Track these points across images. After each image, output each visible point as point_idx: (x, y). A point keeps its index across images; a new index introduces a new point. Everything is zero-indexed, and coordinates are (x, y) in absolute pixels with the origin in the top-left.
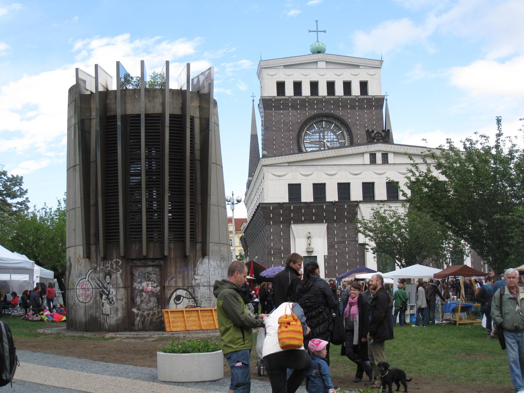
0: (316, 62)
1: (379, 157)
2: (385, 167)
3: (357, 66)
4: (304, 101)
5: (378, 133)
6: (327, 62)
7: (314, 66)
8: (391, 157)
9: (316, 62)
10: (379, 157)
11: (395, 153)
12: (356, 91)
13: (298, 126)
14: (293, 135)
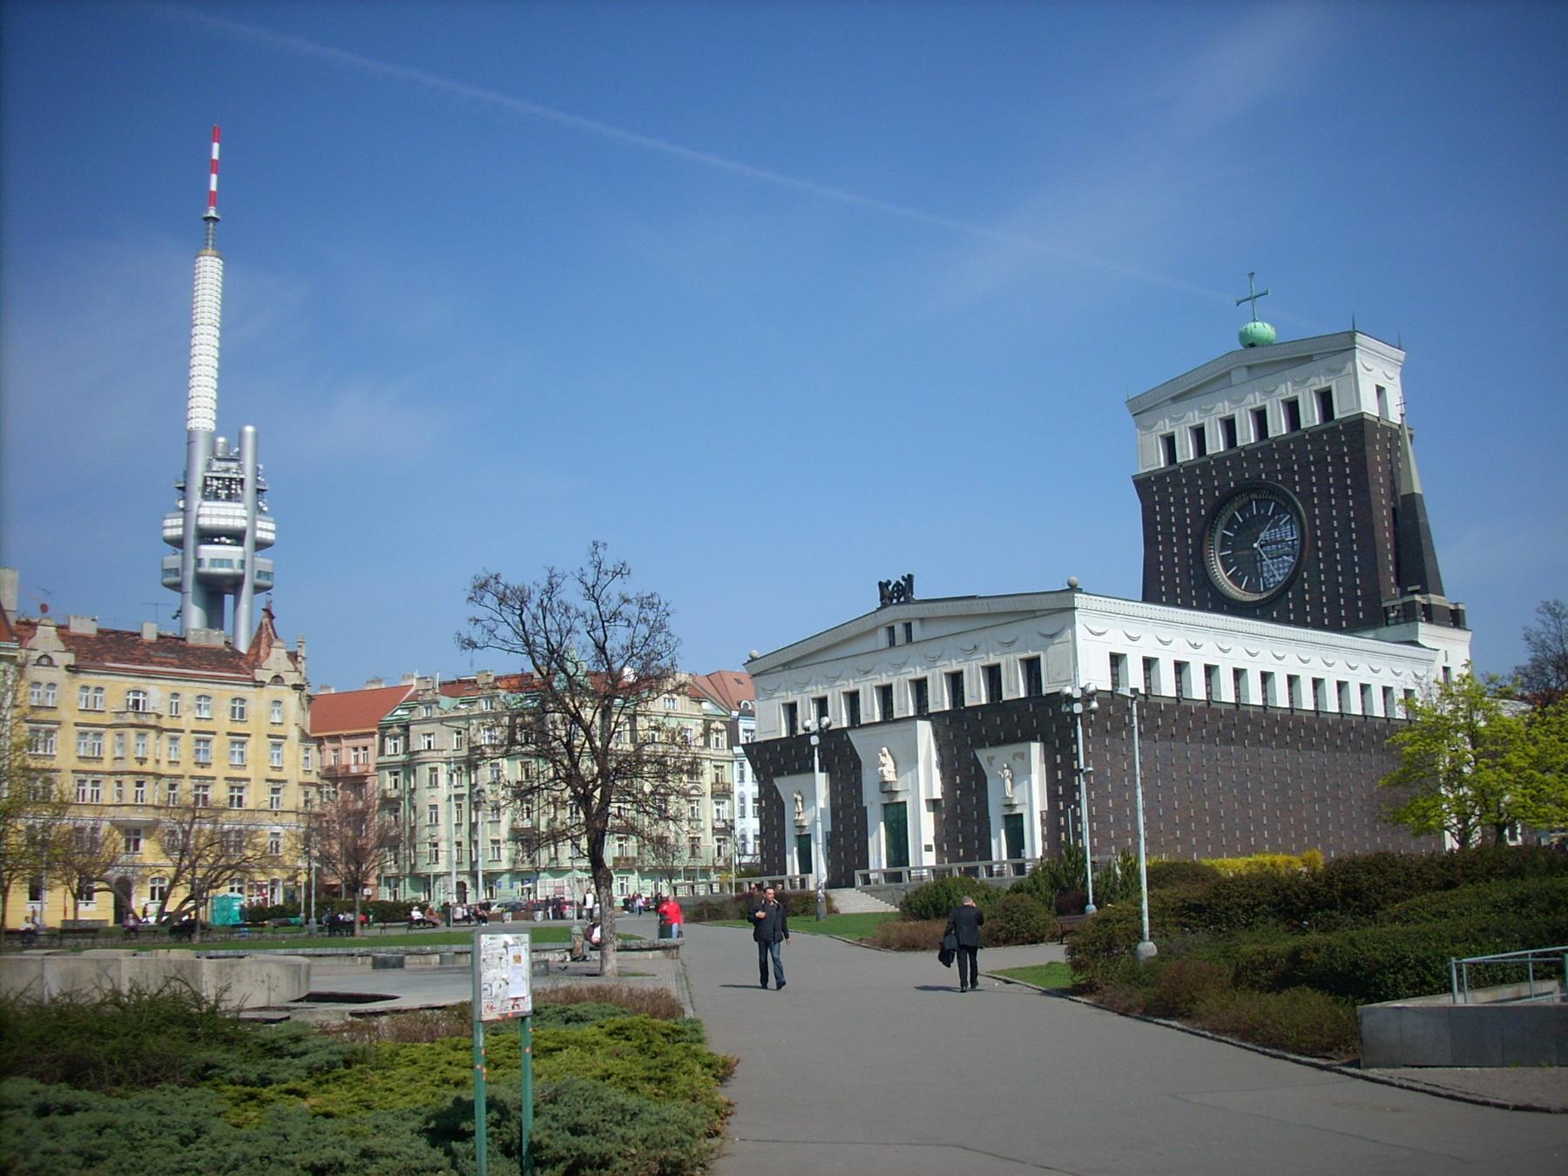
0: (1229, 373)
2: (910, 649)
3: (1308, 359)
6: (1249, 367)
8: (915, 626)
9: (1229, 373)
10: (899, 630)
11: (922, 620)
12: (1311, 416)
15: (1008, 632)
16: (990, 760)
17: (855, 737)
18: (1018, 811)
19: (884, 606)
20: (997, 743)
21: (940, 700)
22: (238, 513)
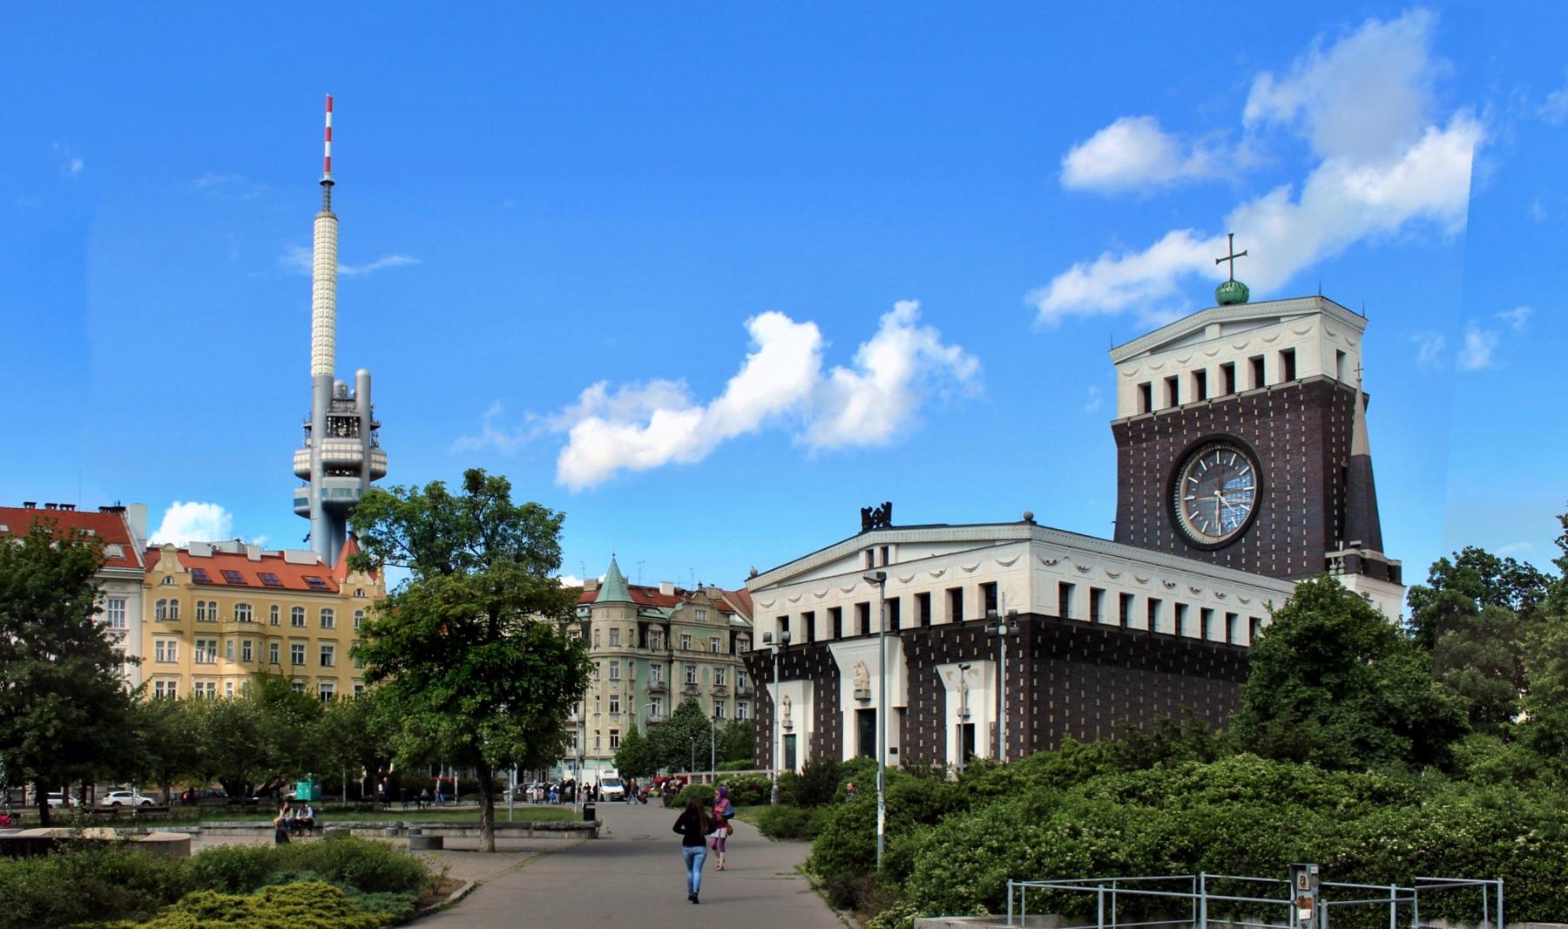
1: (877, 552)
3: (1275, 320)
4: (1176, 416)
5: (878, 511)
7: (1200, 339)
10: (877, 552)
11: (898, 545)
13: (1168, 471)
14: (1160, 490)
15: (971, 559)
16: (949, 674)
17: (835, 649)
18: (970, 721)
19: (865, 531)
20: (955, 659)
21: (908, 619)
22: (355, 447)
